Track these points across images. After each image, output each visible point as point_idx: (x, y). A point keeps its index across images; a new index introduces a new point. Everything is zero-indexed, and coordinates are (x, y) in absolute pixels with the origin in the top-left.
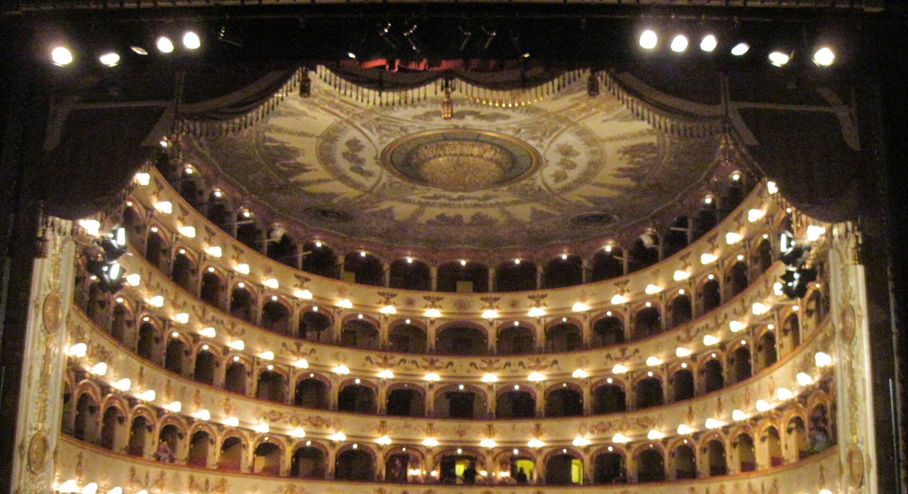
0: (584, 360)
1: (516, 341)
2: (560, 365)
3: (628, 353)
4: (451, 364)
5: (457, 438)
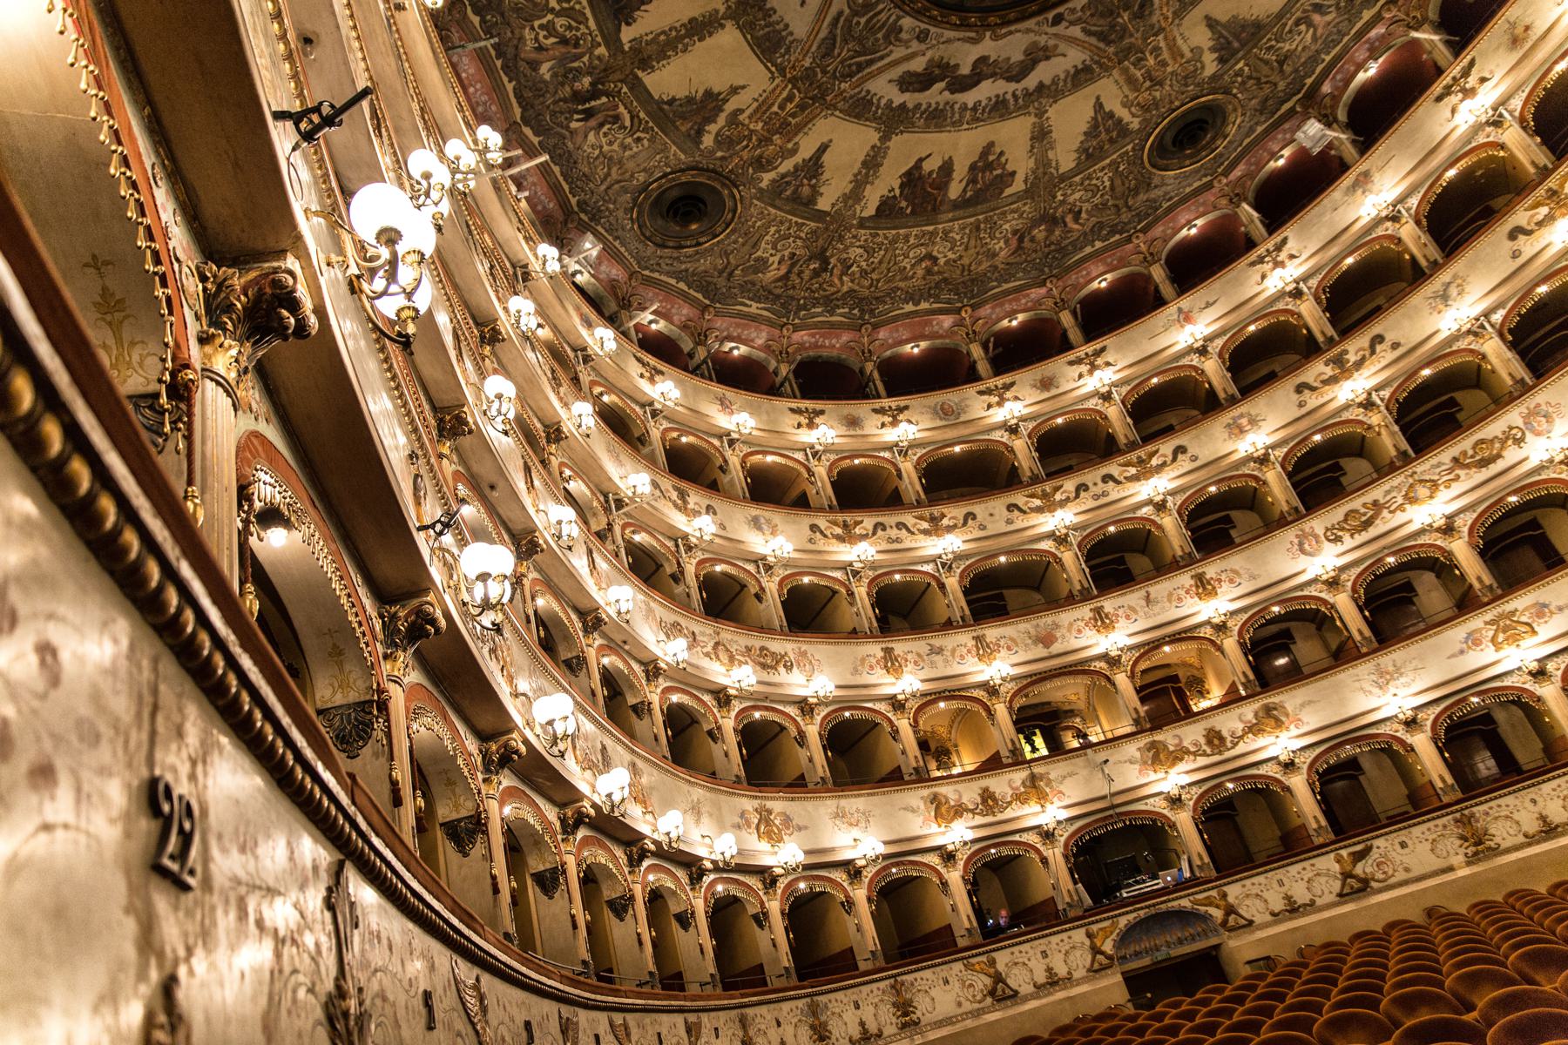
0: (1244, 421)
1: (1071, 446)
3: (1352, 358)
4: (970, 516)
5: (1040, 651)
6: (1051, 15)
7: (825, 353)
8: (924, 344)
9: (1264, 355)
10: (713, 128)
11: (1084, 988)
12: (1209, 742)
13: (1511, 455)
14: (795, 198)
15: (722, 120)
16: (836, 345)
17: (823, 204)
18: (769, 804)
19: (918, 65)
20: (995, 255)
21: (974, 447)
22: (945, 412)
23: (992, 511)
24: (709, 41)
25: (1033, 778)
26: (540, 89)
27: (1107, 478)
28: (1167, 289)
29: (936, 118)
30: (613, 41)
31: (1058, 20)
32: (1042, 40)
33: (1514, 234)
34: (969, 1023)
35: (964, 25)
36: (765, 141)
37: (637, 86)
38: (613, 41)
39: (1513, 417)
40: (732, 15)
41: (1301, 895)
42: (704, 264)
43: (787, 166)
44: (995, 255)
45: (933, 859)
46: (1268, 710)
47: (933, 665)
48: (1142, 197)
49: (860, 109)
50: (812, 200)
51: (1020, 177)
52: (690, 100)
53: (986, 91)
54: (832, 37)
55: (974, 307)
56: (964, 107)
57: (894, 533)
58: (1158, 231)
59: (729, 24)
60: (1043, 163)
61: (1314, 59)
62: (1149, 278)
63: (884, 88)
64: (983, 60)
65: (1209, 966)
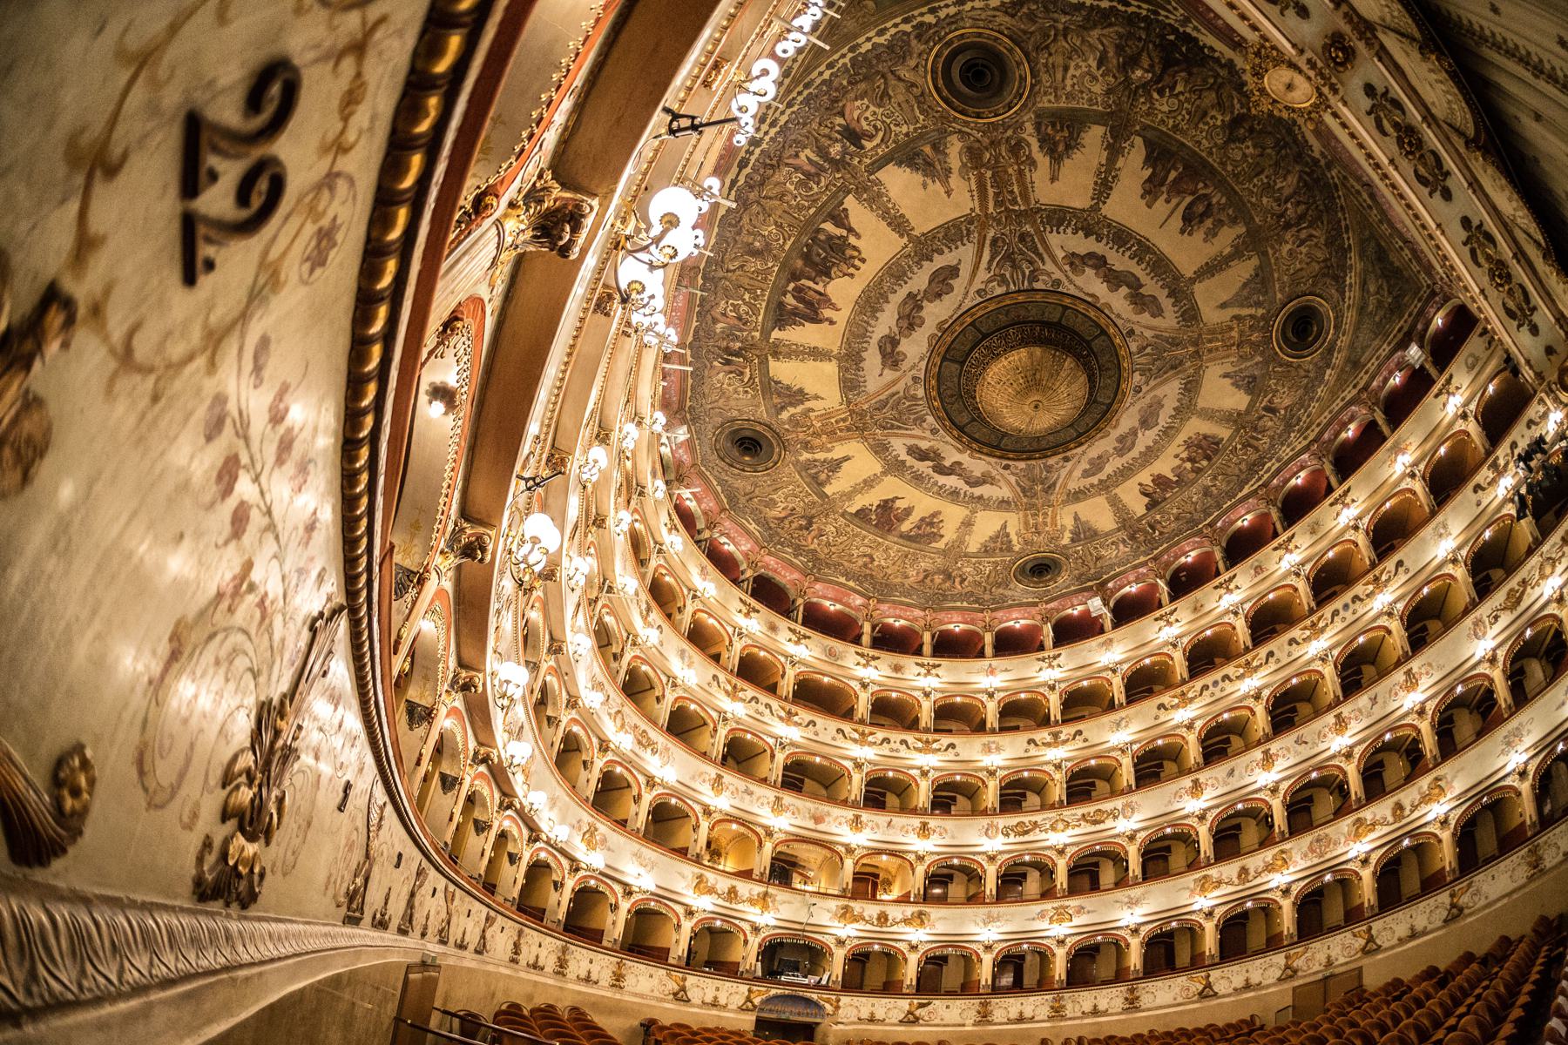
1: (891, 713)
2: (958, 749)
3: (1063, 737)
5: (811, 824)
6: (1005, 462)
7: (778, 578)
8: (839, 607)
9: (1020, 713)
10: (792, 410)
11: (731, 1015)
12: (879, 919)
13: (1109, 823)
14: (815, 477)
15: (800, 409)
16: (786, 577)
17: (828, 490)
18: (598, 825)
19: (924, 445)
20: (907, 577)
21: (836, 683)
22: (831, 653)
23: (827, 726)
24: (818, 363)
25: (766, 894)
26: (710, 334)
27: (904, 742)
28: (989, 650)
29: (918, 479)
30: (766, 334)
31: (1006, 467)
32: (994, 473)
33: (1161, 706)
34: (653, 1003)
35: (959, 439)
36: (816, 435)
37: (764, 363)
38: (766, 334)
39: (1118, 803)
40: (839, 358)
41: (879, 1015)
42: (739, 484)
43: (821, 456)
44: (907, 577)
45: (680, 910)
46: (921, 914)
47: (742, 799)
48: (1001, 590)
49: (880, 449)
50: (822, 484)
51: (944, 541)
52: (788, 388)
53: (952, 481)
54: (884, 404)
55: (879, 601)
56: (936, 483)
57: (761, 708)
58: (999, 614)
59: (834, 362)
60: (960, 541)
61: (1111, 567)
62: (982, 638)
63: (899, 446)
64: (959, 463)
65: (808, 1031)
